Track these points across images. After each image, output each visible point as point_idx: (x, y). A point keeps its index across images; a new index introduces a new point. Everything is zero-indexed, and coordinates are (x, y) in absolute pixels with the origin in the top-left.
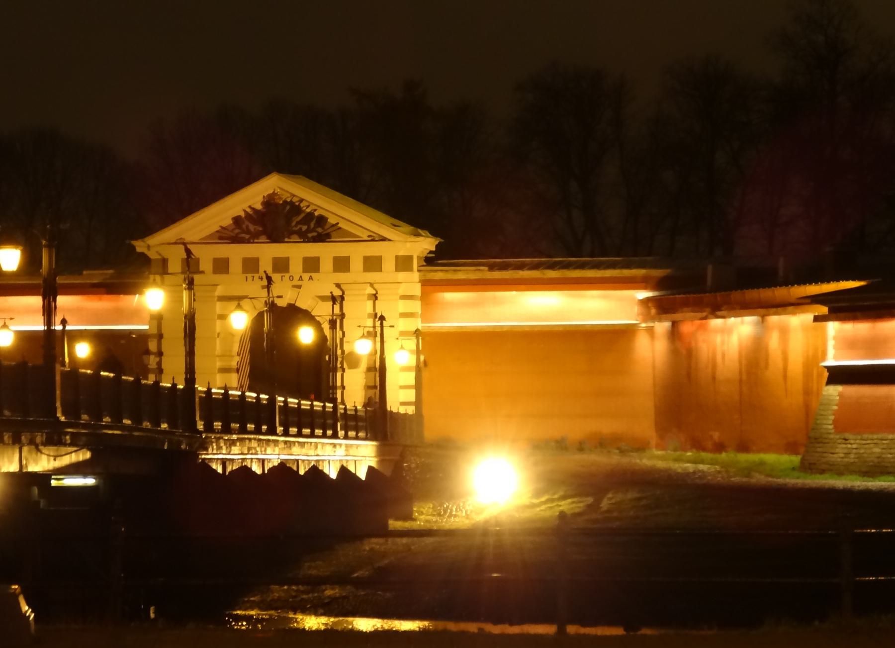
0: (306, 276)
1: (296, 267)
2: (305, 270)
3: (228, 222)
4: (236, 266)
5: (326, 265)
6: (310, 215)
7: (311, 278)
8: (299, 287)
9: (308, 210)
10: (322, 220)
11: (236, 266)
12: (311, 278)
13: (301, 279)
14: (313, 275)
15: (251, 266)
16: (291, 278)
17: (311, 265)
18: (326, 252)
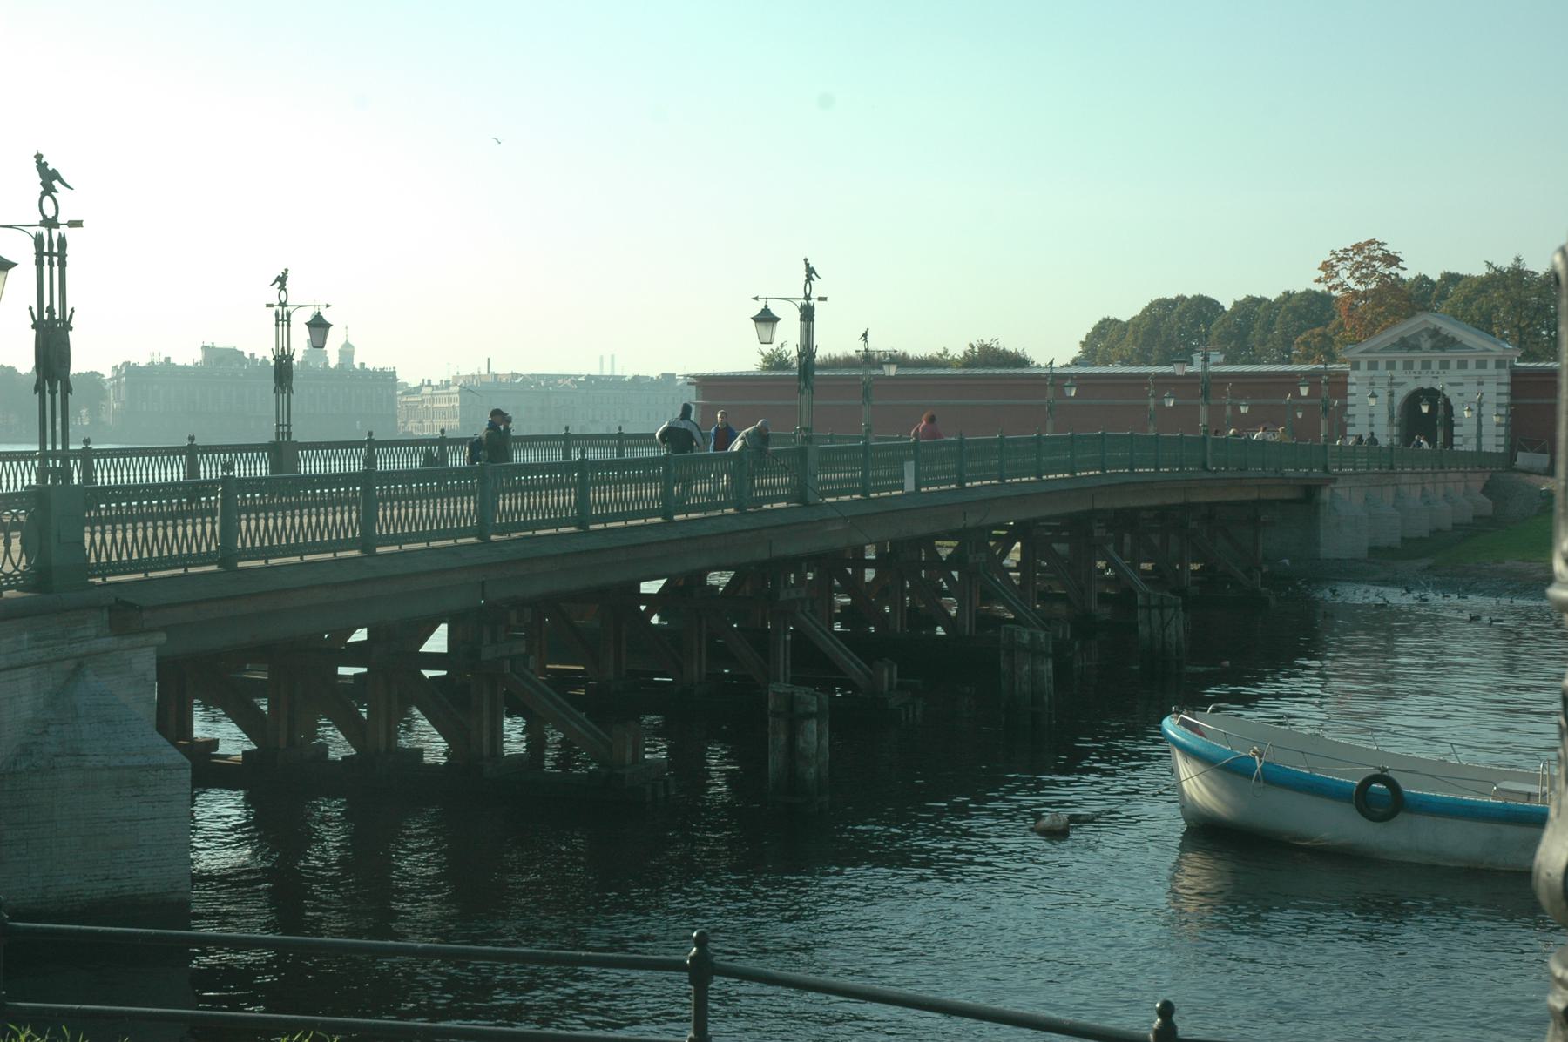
0: (1441, 371)
1: (1435, 366)
2: (1441, 368)
3: (1396, 340)
4: (1399, 365)
5: (1453, 364)
6: (1446, 337)
7: (1444, 373)
8: (1437, 377)
9: (1445, 333)
10: (1454, 339)
11: (1399, 365)
12: (1444, 373)
13: (1438, 373)
14: (1446, 371)
15: (1408, 365)
16: (1433, 373)
17: (1445, 365)
18: (1452, 355)
